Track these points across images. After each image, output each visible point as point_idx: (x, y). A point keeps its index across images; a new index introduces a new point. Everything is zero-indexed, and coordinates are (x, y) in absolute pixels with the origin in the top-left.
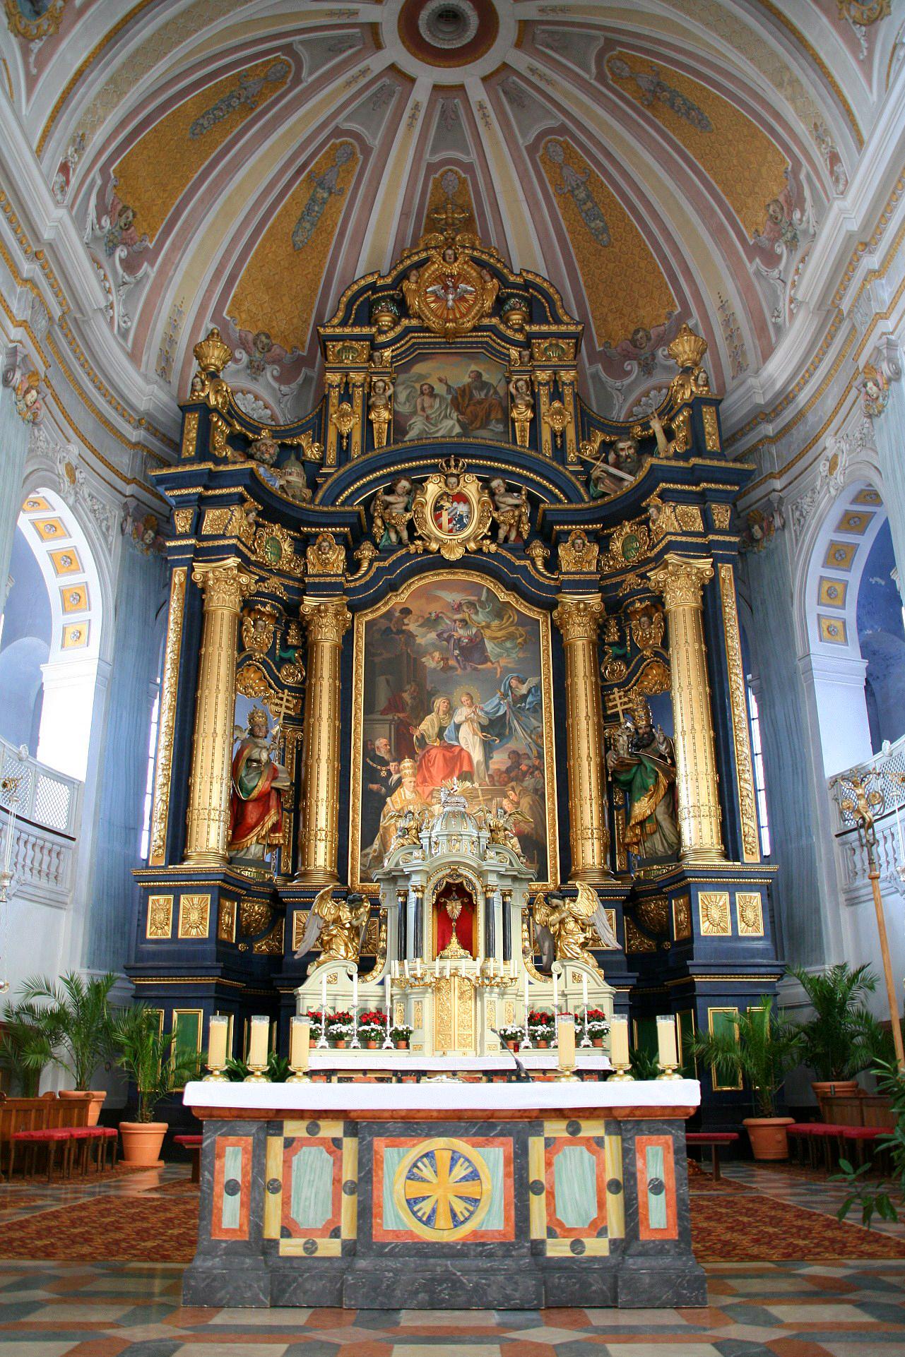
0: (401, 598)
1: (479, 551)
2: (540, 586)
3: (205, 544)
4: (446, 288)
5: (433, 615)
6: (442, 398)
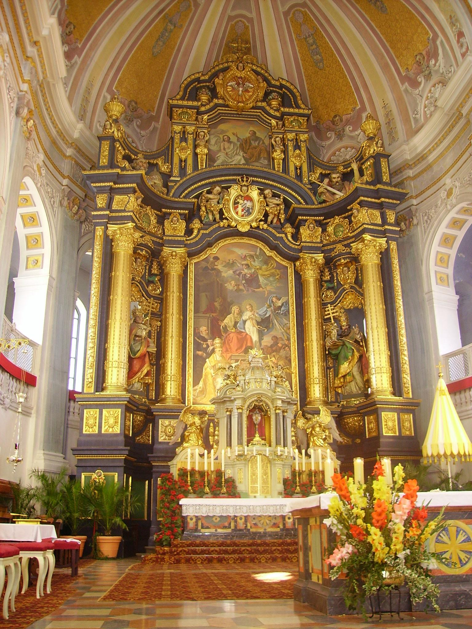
0: (214, 251)
1: (258, 227)
2: (290, 248)
3: (114, 214)
4: (238, 84)
5: (231, 261)
6: (235, 144)
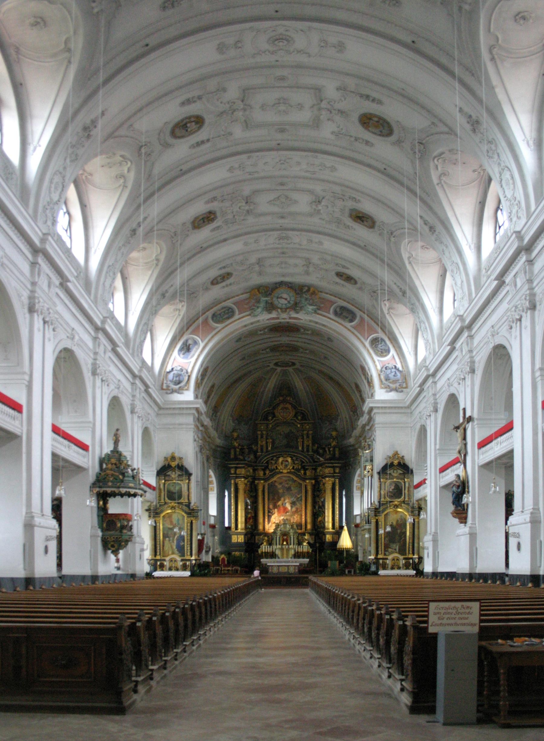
0: (274, 479)
